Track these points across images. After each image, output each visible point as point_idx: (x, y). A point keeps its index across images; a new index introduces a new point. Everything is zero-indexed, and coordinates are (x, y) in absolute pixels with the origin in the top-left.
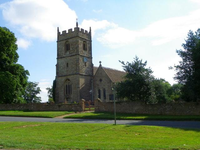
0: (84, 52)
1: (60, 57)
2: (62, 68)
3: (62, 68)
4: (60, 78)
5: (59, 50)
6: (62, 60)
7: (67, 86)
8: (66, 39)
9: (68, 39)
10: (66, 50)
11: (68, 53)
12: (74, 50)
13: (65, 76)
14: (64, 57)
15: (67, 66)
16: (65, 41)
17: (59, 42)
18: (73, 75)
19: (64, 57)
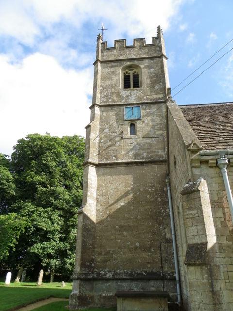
0: (125, 93)
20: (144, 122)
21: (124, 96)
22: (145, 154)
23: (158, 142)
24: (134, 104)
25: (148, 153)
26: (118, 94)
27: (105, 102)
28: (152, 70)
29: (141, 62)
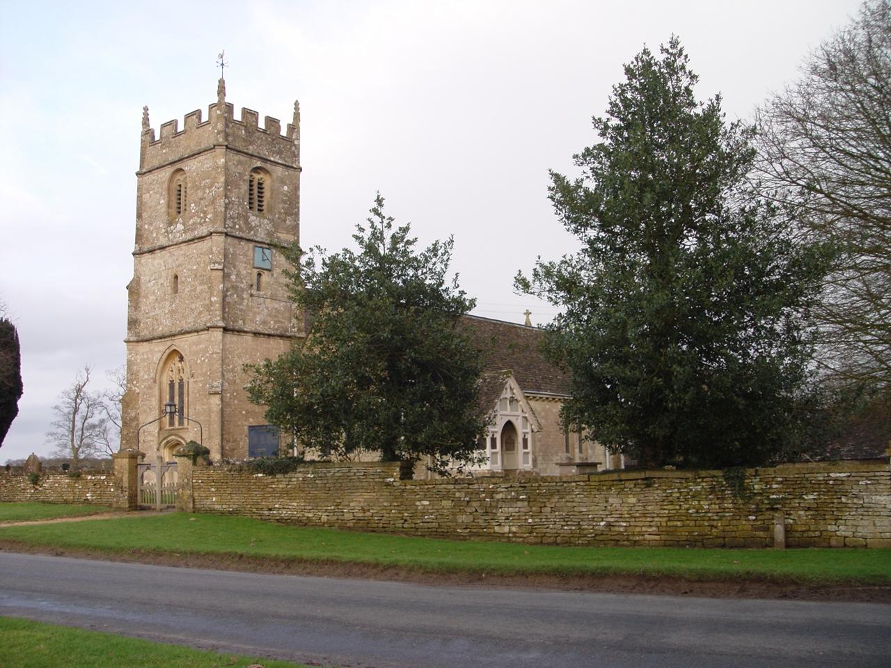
0: (253, 219)
1: (145, 248)
2: (152, 298)
3: (152, 298)
4: (144, 347)
5: (145, 215)
6: (155, 262)
7: (172, 385)
8: (172, 163)
9: (181, 160)
10: (174, 211)
11: (180, 227)
12: (205, 213)
13: (163, 337)
14: (162, 248)
15: (176, 290)
16: (170, 170)
17: (145, 178)
18: (197, 331)
19: (162, 248)
20: (272, 275)
21: (253, 224)
22: (272, 322)
23: (285, 307)
24: (264, 243)
25: (275, 322)
26: (246, 219)
27: (231, 228)
28: (286, 188)
29: (273, 167)
